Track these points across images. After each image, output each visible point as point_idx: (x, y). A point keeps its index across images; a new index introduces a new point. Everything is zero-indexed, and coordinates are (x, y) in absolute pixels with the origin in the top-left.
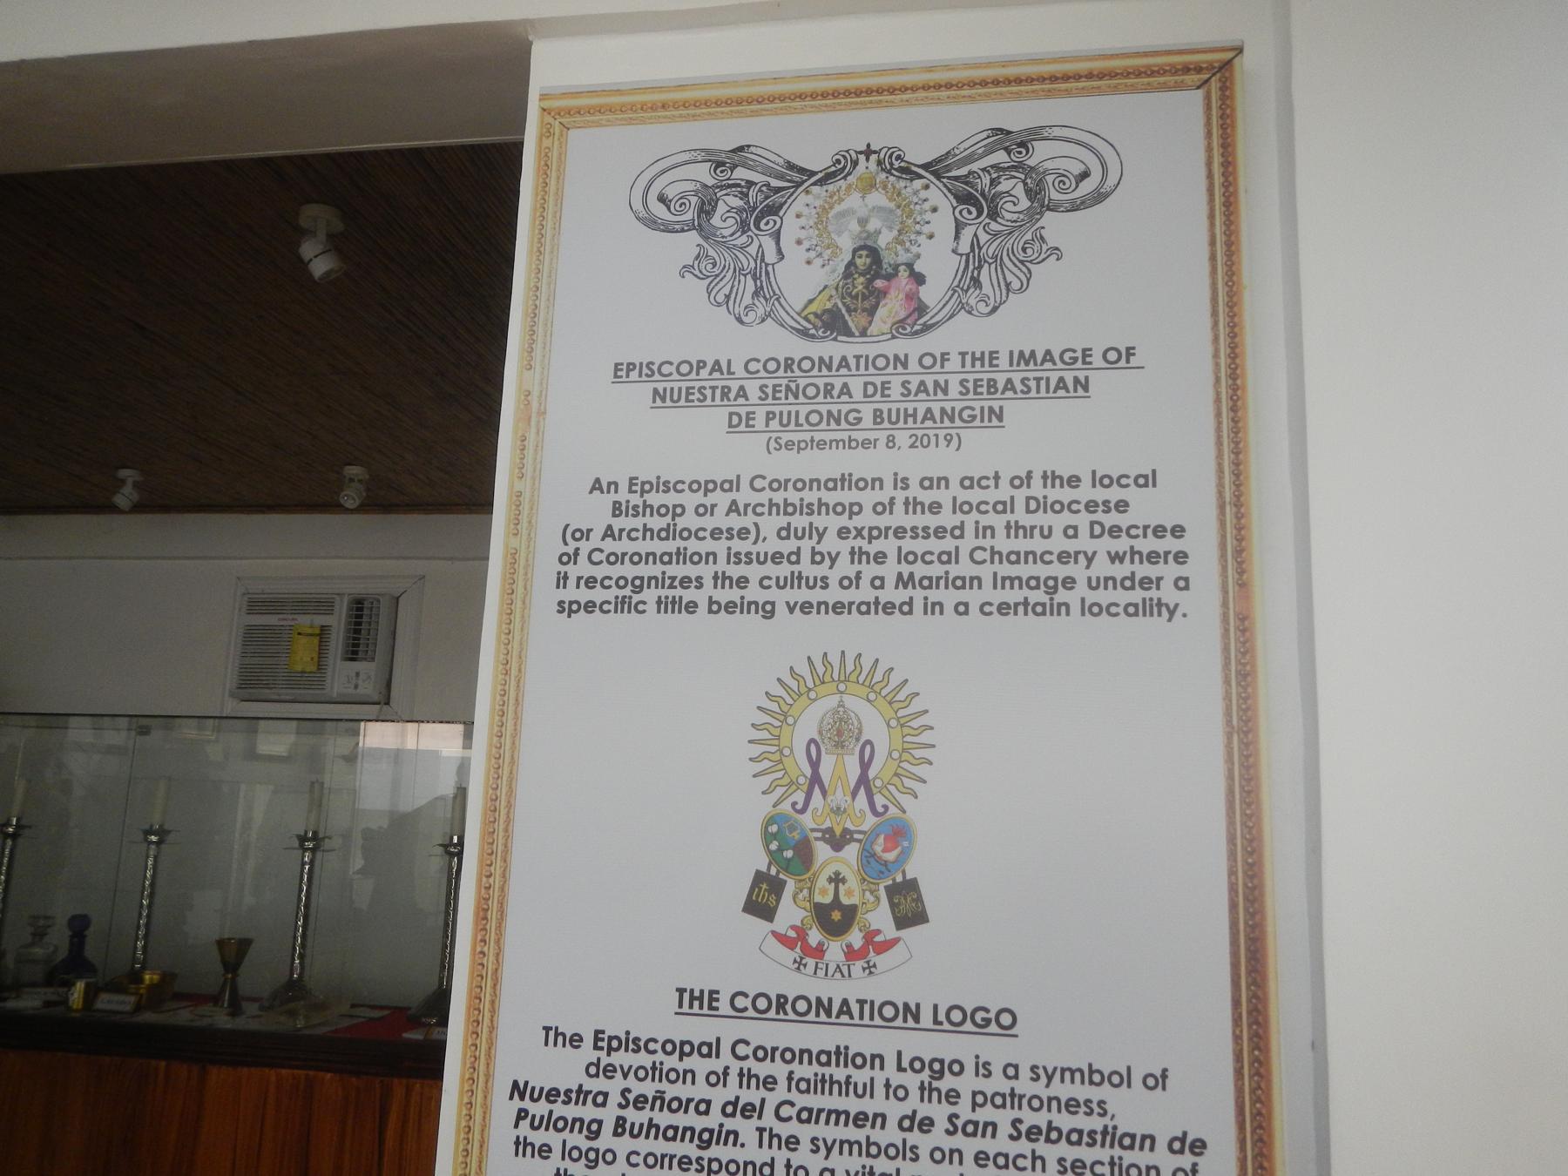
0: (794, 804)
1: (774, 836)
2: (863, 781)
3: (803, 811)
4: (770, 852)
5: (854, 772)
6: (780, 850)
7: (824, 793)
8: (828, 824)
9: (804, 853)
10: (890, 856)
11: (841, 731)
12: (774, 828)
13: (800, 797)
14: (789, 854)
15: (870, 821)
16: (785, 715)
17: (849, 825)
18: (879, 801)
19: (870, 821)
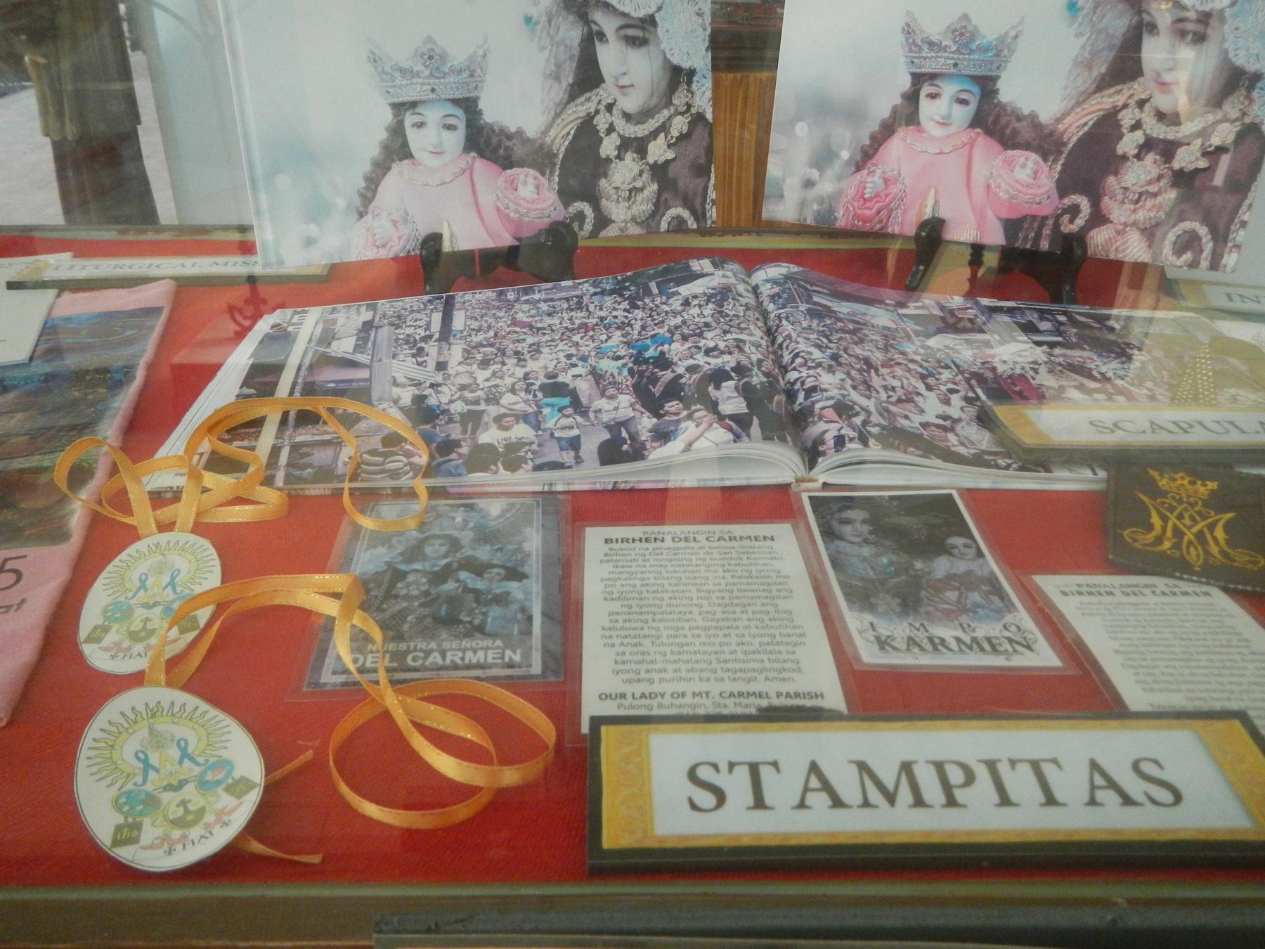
0: (135, 784)
1: (125, 804)
2: (185, 755)
3: (145, 781)
4: (123, 813)
5: (175, 753)
6: (132, 808)
7: (157, 770)
8: (165, 783)
9: (152, 802)
10: (220, 776)
11: (157, 739)
12: (123, 800)
13: (139, 779)
14: (141, 807)
15: (197, 770)
16: (112, 746)
17: (182, 777)
18: (201, 760)
19: (197, 770)
